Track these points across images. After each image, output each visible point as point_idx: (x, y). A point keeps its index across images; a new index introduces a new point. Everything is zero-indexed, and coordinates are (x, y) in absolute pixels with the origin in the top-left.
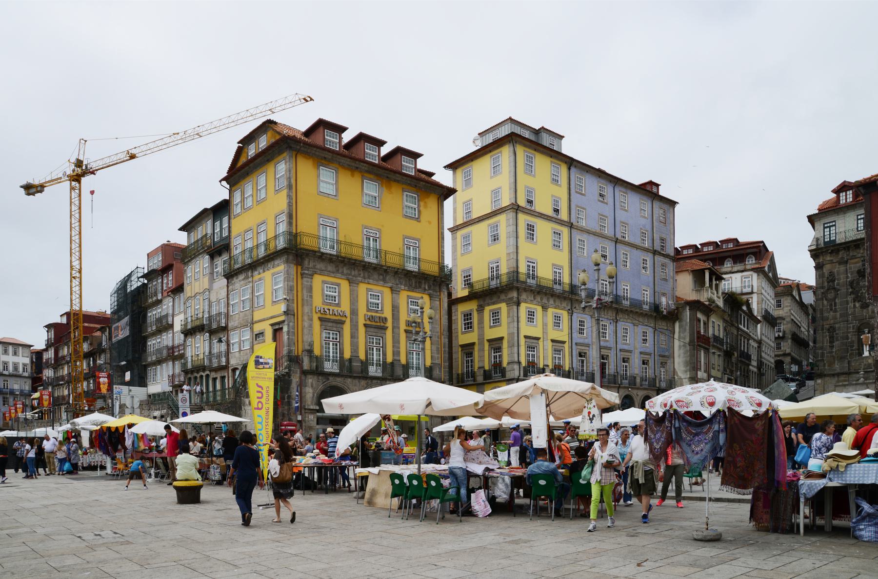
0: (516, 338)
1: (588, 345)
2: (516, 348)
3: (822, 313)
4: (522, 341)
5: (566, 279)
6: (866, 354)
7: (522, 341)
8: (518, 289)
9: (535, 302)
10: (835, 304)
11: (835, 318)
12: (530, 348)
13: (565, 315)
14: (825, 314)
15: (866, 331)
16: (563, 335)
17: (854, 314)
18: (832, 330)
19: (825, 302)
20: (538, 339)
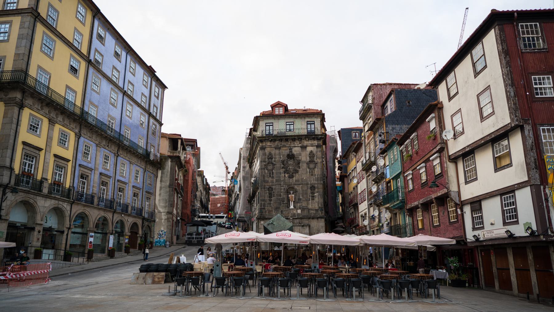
0: (11, 141)
1: (91, 170)
2: (9, 152)
3: (264, 177)
4: (19, 148)
5: (79, 103)
6: (292, 207)
7: (19, 148)
8: (23, 92)
9: (42, 112)
10: (273, 173)
11: (272, 182)
12: (26, 156)
13: (72, 136)
14: (266, 179)
15: (292, 192)
16: (68, 154)
17: (284, 180)
18: (270, 189)
19: (266, 171)
20: (40, 150)
